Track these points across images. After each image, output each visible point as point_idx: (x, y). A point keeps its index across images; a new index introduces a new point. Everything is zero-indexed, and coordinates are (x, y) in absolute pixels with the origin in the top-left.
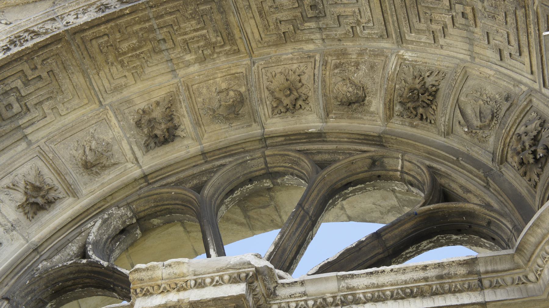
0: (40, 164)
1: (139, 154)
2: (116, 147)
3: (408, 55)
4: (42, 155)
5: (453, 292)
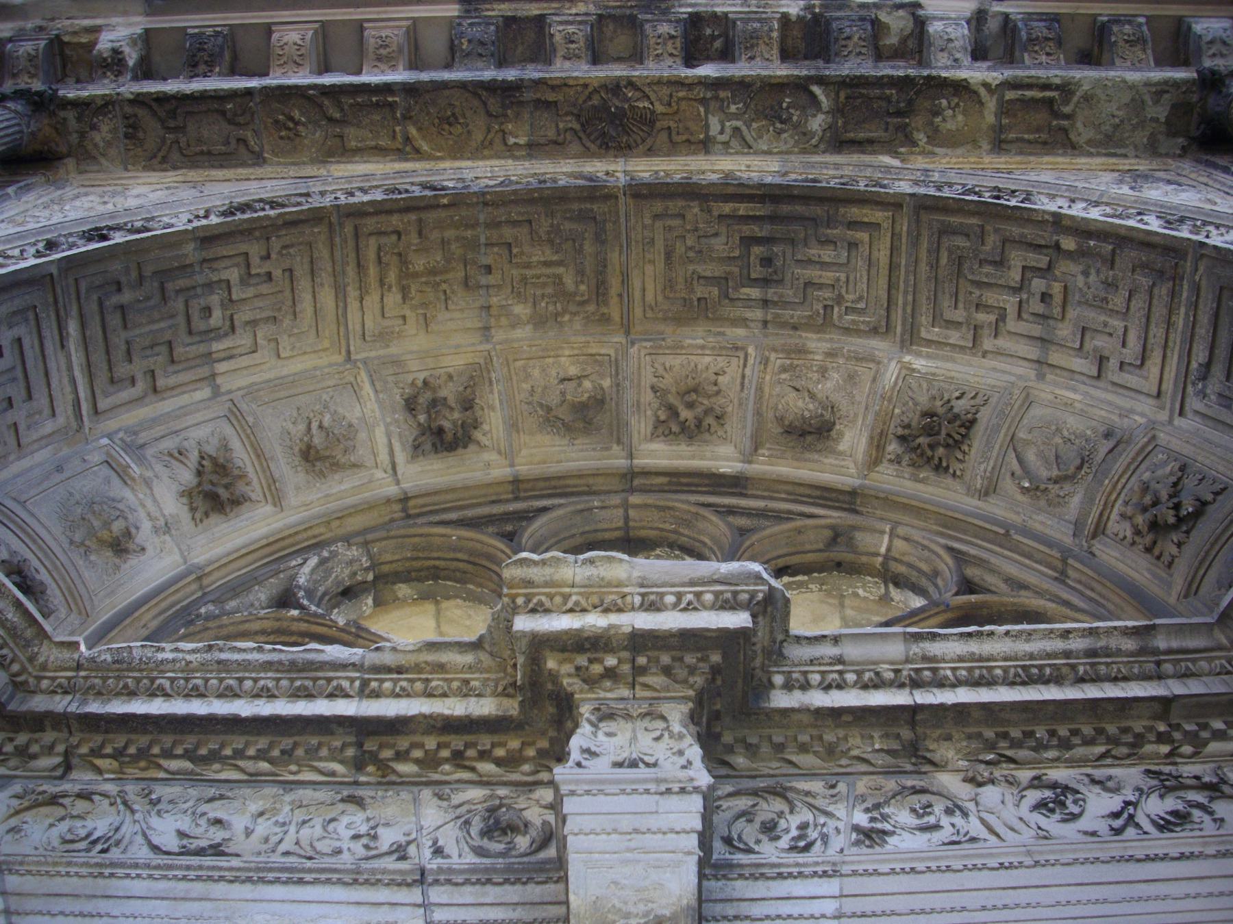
0: (228, 430)
1: (400, 457)
2: (362, 435)
3: (919, 364)
4: (234, 415)
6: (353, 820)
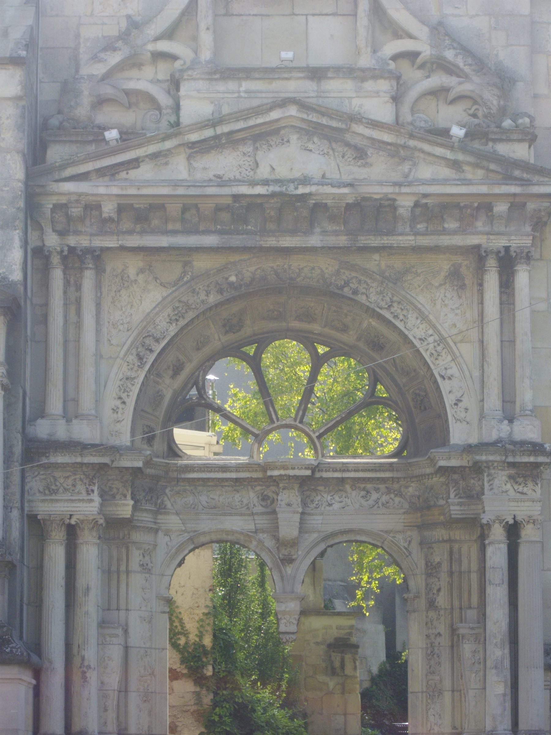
3: (374, 323)
5: (383, 471)
6: (237, 497)
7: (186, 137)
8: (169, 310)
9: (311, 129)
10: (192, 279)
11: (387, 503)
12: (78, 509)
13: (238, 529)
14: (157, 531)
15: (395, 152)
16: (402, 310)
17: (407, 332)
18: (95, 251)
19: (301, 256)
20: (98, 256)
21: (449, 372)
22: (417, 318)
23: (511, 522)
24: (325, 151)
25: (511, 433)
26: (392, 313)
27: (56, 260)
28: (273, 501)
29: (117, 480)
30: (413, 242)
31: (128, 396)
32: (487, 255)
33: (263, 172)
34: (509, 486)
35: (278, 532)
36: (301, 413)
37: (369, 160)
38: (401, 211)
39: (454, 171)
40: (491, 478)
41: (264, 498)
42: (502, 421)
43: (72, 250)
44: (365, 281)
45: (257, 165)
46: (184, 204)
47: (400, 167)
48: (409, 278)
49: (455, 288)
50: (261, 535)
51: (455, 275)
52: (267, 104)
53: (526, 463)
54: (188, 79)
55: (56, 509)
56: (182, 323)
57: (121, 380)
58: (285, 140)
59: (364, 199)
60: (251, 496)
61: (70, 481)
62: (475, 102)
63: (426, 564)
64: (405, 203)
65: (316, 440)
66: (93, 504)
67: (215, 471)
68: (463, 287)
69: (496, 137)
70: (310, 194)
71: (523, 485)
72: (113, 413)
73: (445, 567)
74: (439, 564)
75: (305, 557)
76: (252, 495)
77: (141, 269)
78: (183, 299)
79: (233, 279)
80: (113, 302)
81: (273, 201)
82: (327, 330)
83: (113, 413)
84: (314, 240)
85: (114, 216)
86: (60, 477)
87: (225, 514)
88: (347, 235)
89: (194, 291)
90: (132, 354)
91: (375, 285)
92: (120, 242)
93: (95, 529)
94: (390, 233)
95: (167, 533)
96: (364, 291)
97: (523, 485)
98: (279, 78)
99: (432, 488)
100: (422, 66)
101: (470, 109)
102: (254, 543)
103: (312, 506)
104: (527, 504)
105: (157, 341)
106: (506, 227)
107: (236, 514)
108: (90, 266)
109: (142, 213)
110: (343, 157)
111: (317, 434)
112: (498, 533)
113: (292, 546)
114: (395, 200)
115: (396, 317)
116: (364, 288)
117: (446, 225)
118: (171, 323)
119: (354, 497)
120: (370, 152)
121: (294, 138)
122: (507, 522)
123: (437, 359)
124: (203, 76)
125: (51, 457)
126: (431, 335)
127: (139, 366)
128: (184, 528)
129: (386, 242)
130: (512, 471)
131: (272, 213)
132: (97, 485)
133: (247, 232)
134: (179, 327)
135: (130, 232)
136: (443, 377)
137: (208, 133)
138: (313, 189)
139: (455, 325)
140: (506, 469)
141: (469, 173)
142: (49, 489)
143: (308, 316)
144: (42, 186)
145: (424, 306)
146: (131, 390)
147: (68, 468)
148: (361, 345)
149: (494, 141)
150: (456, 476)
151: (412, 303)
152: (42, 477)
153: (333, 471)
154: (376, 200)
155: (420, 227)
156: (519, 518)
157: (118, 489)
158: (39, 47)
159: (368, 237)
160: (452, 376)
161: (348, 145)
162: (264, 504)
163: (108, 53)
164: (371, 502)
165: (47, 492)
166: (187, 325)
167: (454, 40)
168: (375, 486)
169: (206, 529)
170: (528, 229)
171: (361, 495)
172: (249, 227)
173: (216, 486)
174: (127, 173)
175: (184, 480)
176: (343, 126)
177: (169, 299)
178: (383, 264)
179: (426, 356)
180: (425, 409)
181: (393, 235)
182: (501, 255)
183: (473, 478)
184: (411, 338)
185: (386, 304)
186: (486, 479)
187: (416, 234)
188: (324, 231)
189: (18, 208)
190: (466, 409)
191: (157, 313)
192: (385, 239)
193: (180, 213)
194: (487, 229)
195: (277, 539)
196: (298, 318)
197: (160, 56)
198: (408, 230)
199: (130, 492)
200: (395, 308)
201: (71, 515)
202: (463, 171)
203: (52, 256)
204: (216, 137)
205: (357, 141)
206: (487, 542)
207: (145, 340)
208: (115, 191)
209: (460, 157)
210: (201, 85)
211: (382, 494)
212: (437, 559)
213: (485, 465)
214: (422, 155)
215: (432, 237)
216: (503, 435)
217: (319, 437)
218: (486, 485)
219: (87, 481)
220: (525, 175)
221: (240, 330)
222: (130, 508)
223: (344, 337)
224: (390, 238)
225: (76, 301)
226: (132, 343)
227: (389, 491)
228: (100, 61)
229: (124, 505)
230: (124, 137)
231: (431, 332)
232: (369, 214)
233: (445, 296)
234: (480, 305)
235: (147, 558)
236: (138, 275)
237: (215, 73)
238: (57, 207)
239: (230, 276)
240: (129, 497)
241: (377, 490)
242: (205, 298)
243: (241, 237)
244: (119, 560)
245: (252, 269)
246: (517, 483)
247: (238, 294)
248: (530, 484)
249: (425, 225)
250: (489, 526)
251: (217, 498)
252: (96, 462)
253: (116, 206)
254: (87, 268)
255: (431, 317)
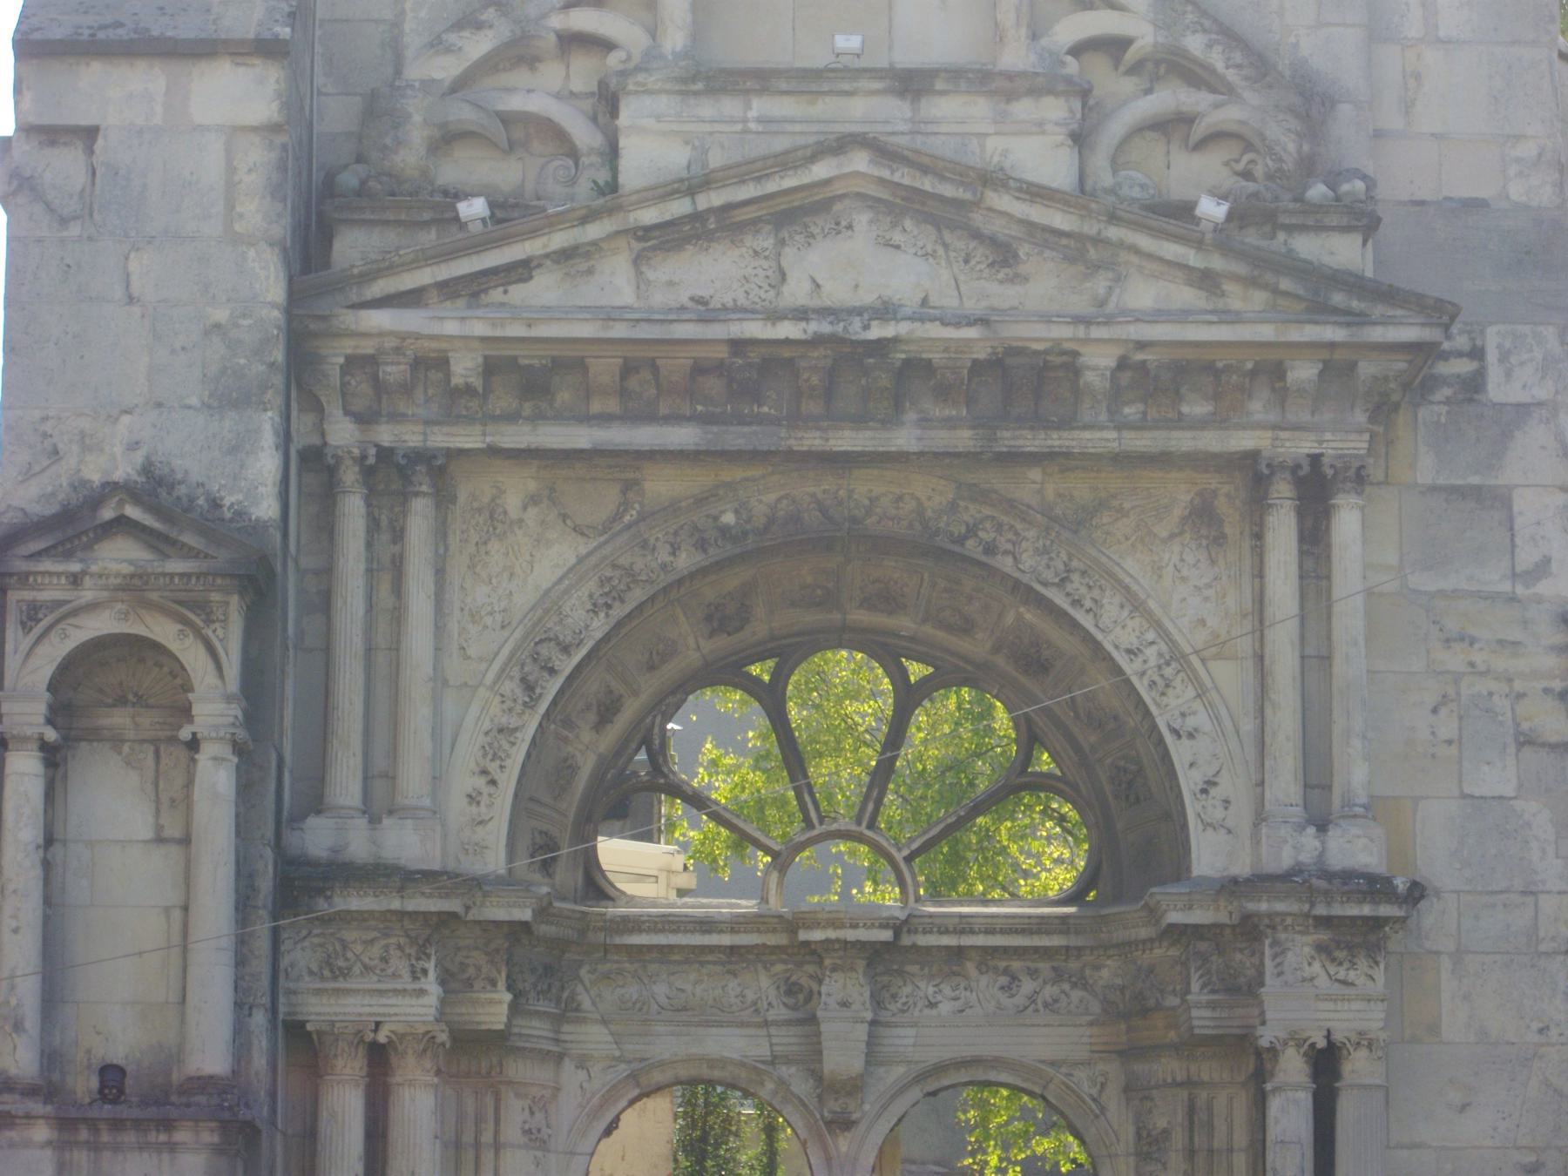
3: (1028, 616)
5: (1048, 933)
6: (733, 985)
7: (632, 217)
8: (591, 585)
9: (898, 201)
10: (642, 518)
11: (1056, 1001)
12: (392, 1011)
13: (735, 1056)
14: (559, 1058)
15: (1078, 252)
16: (1090, 587)
17: (1099, 637)
18: (434, 457)
19: (876, 472)
20: (439, 469)
21: (1191, 722)
22: (1122, 606)
23: (1321, 1043)
24: (929, 248)
25: (1322, 854)
26: (1068, 594)
27: (350, 475)
28: (809, 999)
29: (477, 948)
30: (1115, 444)
31: (502, 767)
32: (1272, 474)
33: (797, 292)
34: (1317, 967)
35: (820, 1062)
36: (871, 806)
37: (1022, 269)
38: (1089, 377)
39: (1203, 294)
40: (1277, 949)
41: (791, 989)
42: (1304, 829)
43: (385, 454)
44: (1012, 527)
45: (783, 276)
46: (625, 359)
47: (1088, 285)
48: (1105, 520)
49: (1204, 542)
50: (784, 1068)
51: (1203, 516)
52: (805, 147)
53: (1353, 919)
54: (636, 92)
55: (347, 1010)
56: (619, 611)
57: (487, 733)
58: (844, 223)
59: (1012, 351)
60: (762, 985)
61: (376, 950)
62: (1249, 147)
63: (1138, 1134)
64: (1099, 361)
65: (903, 866)
66: (426, 1000)
67: (686, 931)
68: (1220, 540)
69: (1294, 221)
70: (896, 340)
71: (1346, 965)
72: (470, 804)
73: (1178, 1139)
74: (1166, 1133)
75: (879, 1115)
76: (765, 981)
77: (532, 497)
78: (621, 561)
79: (729, 518)
80: (472, 567)
81: (816, 354)
82: (928, 629)
83: (470, 804)
84: (904, 439)
85: (477, 382)
86: (355, 942)
87: (708, 1024)
88: (974, 428)
89: (644, 544)
90: (512, 678)
91: (1031, 534)
92: (488, 439)
93: (429, 1053)
94: (1065, 424)
95: (582, 1063)
96: (1009, 547)
97: (1346, 965)
98: (830, 93)
99: (1151, 970)
100: (1136, 69)
101: (1237, 161)
102: (770, 1086)
103: (893, 1007)
104: (1356, 1006)
105: (566, 650)
106: (1313, 413)
107: (730, 1024)
108: (424, 488)
109: (532, 377)
110: (966, 262)
111: (906, 852)
112: (1293, 1067)
113: (849, 1094)
114: (1076, 354)
115: (1077, 603)
116: (1009, 541)
117: (1185, 409)
118: (596, 613)
119: (985, 989)
120: (1023, 250)
121: (862, 219)
122: (1313, 1045)
123: (1163, 694)
124: (668, 86)
125: (337, 900)
126: (1152, 643)
127: (525, 704)
128: (617, 1053)
129: (1057, 443)
130: (1324, 936)
131: (815, 380)
132: (433, 958)
133: (760, 420)
134: (613, 621)
135: (512, 418)
136: (1176, 733)
137: (679, 207)
138: (903, 329)
139: (1202, 622)
140: (1312, 930)
141: (1235, 297)
142: (329, 965)
143: (888, 600)
144: (324, 318)
145: (1138, 583)
146: (508, 756)
147: (373, 923)
148: (1000, 661)
149: (1290, 229)
150: (1203, 946)
151: (1111, 575)
152: (316, 940)
153: (940, 933)
154: (1036, 353)
155: (1131, 411)
156: (1338, 1037)
157: (479, 969)
158: (318, 16)
159: (1017, 433)
160: (1196, 730)
161: (977, 235)
162: (791, 1001)
163: (466, 34)
164: (1020, 1000)
165: (327, 973)
166: (630, 616)
167: (1204, 13)
168: (1030, 964)
169: (666, 1056)
170: (1360, 417)
171: (998, 985)
172: (765, 409)
173: (687, 961)
174: (506, 292)
175: (619, 948)
176: (968, 196)
177: (593, 560)
178: (1050, 493)
179: (1141, 687)
180: (1138, 800)
181: (1073, 429)
182: (1301, 473)
183: (1241, 950)
184: (1109, 648)
185: (1057, 574)
186: (1268, 952)
187: (1119, 428)
188: (927, 420)
189: (272, 365)
190: (1227, 802)
191: (566, 592)
192: (1055, 436)
193: (617, 379)
194: (1273, 417)
195: (819, 1078)
196: (867, 603)
197: (573, 42)
198: (1103, 417)
199: (504, 975)
200: (1076, 585)
201: (378, 1024)
202: (1223, 295)
203: (343, 468)
204: (696, 217)
205: (997, 227)
206: (1269, 1086)
207: (539, 648)
208: (479, 329)
209: (1217, 263)
210: (664, 103)
211: (1045, 982)
212: (1162, 1123)
213: (1266, 921)
214: (1134, 259)
215: (1156, 433)
216: (1306, 857)
217: (909, 859)
218: (1269, 964)
219: (413, 951)
220: (1355, 304)
221: (741, 628)
222: (504, 1009)
223: (963, 645)
224: (1065, 434)
225: (393, 562)
226: (512, 654)
227: (1059, 976)
228: (449, 50)
229: (491, 1002)
230: (500, 214)
231: (1151, 636)
232: (1023, 382)
233: (1182, 560)
234: (1257, 580)
235: (539, 1116)
236: (525, 508)
237: (694, 79)
238: (353, 363)
239: (723, 512)
240: (502, 985)
241: (1033, 974)
242: (669, 559)
243: (746, 429)
244: (479, 1119)
245: (771, 497)
246: (1333, 960)
247: (738, 551)
248: (1363, 963)
249: (1141, 407)
250: (1273, 1051)
251: (689, 988)
252: (433, 909)
253: (480, 360)
254: (417, 494)
255: (1152, 604)
